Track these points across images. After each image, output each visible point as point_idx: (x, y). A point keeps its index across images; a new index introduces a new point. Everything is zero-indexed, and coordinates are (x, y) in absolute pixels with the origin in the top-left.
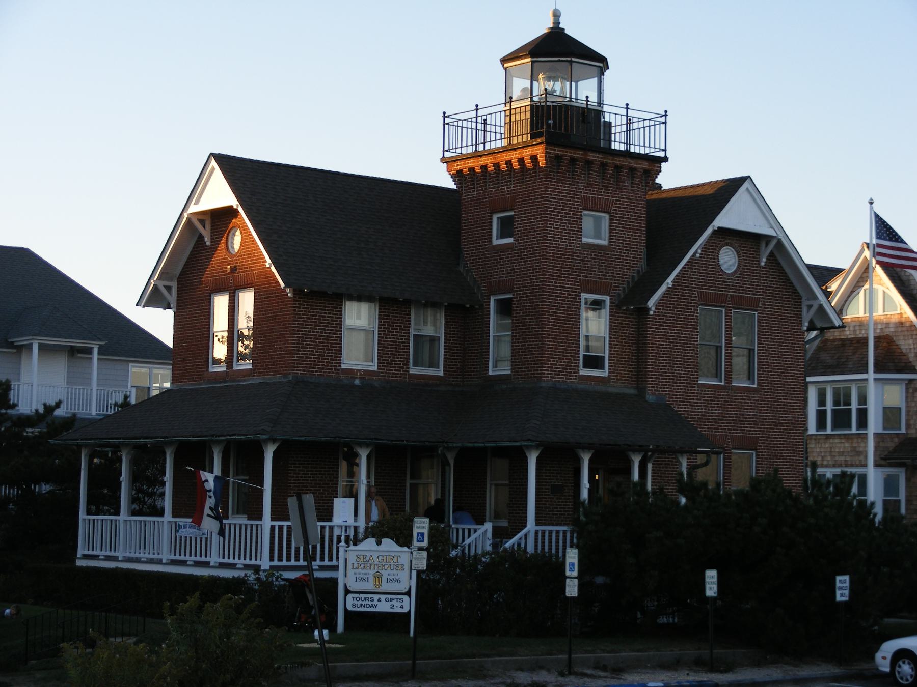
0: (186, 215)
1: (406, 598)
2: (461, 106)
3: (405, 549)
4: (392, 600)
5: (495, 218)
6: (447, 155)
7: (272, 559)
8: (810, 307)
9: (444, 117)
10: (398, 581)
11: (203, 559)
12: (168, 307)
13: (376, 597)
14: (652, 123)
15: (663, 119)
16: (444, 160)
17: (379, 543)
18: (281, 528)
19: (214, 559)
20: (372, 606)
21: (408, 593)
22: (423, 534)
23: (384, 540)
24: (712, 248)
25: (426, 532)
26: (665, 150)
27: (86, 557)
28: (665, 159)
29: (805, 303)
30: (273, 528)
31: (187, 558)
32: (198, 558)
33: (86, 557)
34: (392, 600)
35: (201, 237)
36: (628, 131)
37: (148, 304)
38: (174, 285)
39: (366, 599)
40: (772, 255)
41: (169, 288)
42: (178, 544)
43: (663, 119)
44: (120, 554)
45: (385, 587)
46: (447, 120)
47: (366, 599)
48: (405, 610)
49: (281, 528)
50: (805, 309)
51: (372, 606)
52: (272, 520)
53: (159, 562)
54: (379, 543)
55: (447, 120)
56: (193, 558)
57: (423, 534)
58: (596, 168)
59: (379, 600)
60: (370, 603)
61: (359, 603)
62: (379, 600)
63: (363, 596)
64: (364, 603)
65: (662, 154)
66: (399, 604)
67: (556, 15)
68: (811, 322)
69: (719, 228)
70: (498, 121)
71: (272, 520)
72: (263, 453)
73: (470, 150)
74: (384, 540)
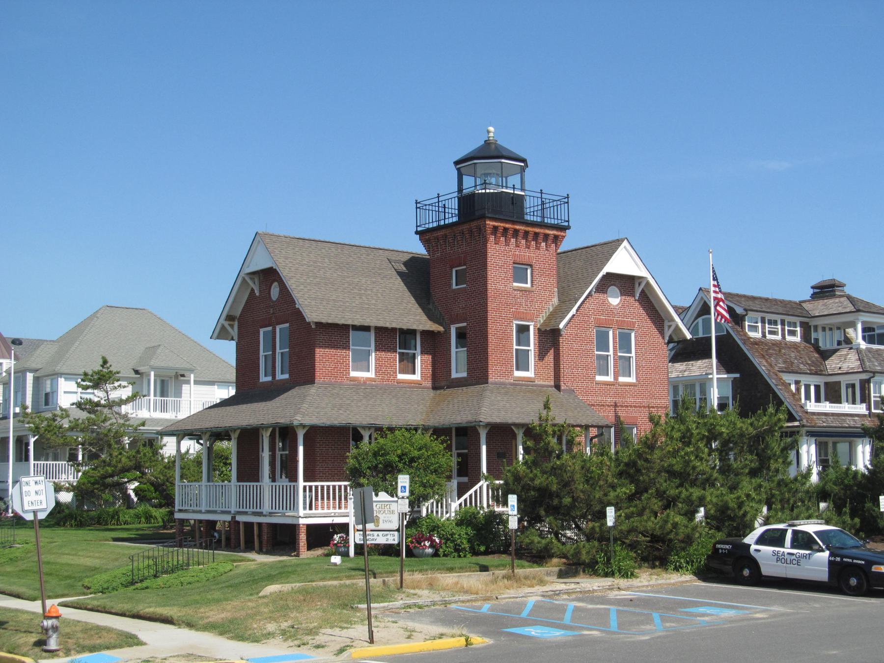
0: (242, 274)
1: (396, 533)
2: (427, 195)
6: (419, 229)
7: (305, 508)
8: (670, 326)
11: (258, 510)
12: (232, 339)
13: (376, 533)
14: (559, 203)
15: (566, 200)
16: (417, 233)
19: (203, 509)
21: (398, 530)
22: (405, 487)
24: (602, 287)
25: (407, 485)
26: (568, 221)
27: (180, 511)
28: (568, 228)
29: (666, 324)
30: (305, 487)
31: (248, 510)
32: (255, 510)
33: (180, 511)
35: (253, 290)
36: (543, 209)
37: (218, 337)
38: (236, 324)
40: (643, 292)
41: (232, 326)
42: (240, 501)
43: (566, 200)
44: (203, 509)
45: (381, 527)
46: (419, 205)
48: (396, 542)
49: (311, 487)
50: (666, 328)
52: (305, 481)
53: (200, 512)
55: (419, 205)
56: (251, 510)
57: (405, 487)
58: (521, 234)
65: (566, 224)
68: (670, 337)
69: (607, 273)
70: (454, 205)
71: (305, 481)
72: (296, 435)
73: (435, 225)
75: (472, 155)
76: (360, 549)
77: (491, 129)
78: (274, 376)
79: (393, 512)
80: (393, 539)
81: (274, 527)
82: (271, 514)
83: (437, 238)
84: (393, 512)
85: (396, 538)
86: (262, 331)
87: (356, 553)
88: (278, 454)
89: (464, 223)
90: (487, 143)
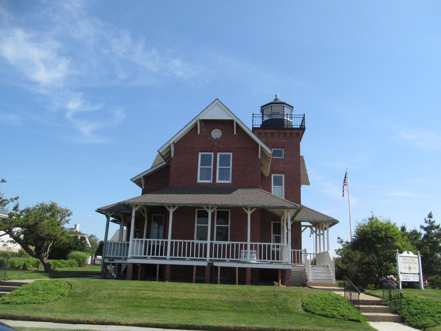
0: (198, 119)
1: (418, 275)
3: (416, 256)
10: (415, 268)
13: (409, 275)
17: (408, 253)
21: (419, 274)
34: (414, 276)
39: (407, 276)
47: (407, 276)
48: (418, 281)
54: (408, 253)
61: (405, 278)
63: (405, 275)
64: (406, 278)
78: (214, 179)
79: (415, 263)
84: (415, 263)
85: (418, 278)
86: (200, 154)
88: (216, 226)
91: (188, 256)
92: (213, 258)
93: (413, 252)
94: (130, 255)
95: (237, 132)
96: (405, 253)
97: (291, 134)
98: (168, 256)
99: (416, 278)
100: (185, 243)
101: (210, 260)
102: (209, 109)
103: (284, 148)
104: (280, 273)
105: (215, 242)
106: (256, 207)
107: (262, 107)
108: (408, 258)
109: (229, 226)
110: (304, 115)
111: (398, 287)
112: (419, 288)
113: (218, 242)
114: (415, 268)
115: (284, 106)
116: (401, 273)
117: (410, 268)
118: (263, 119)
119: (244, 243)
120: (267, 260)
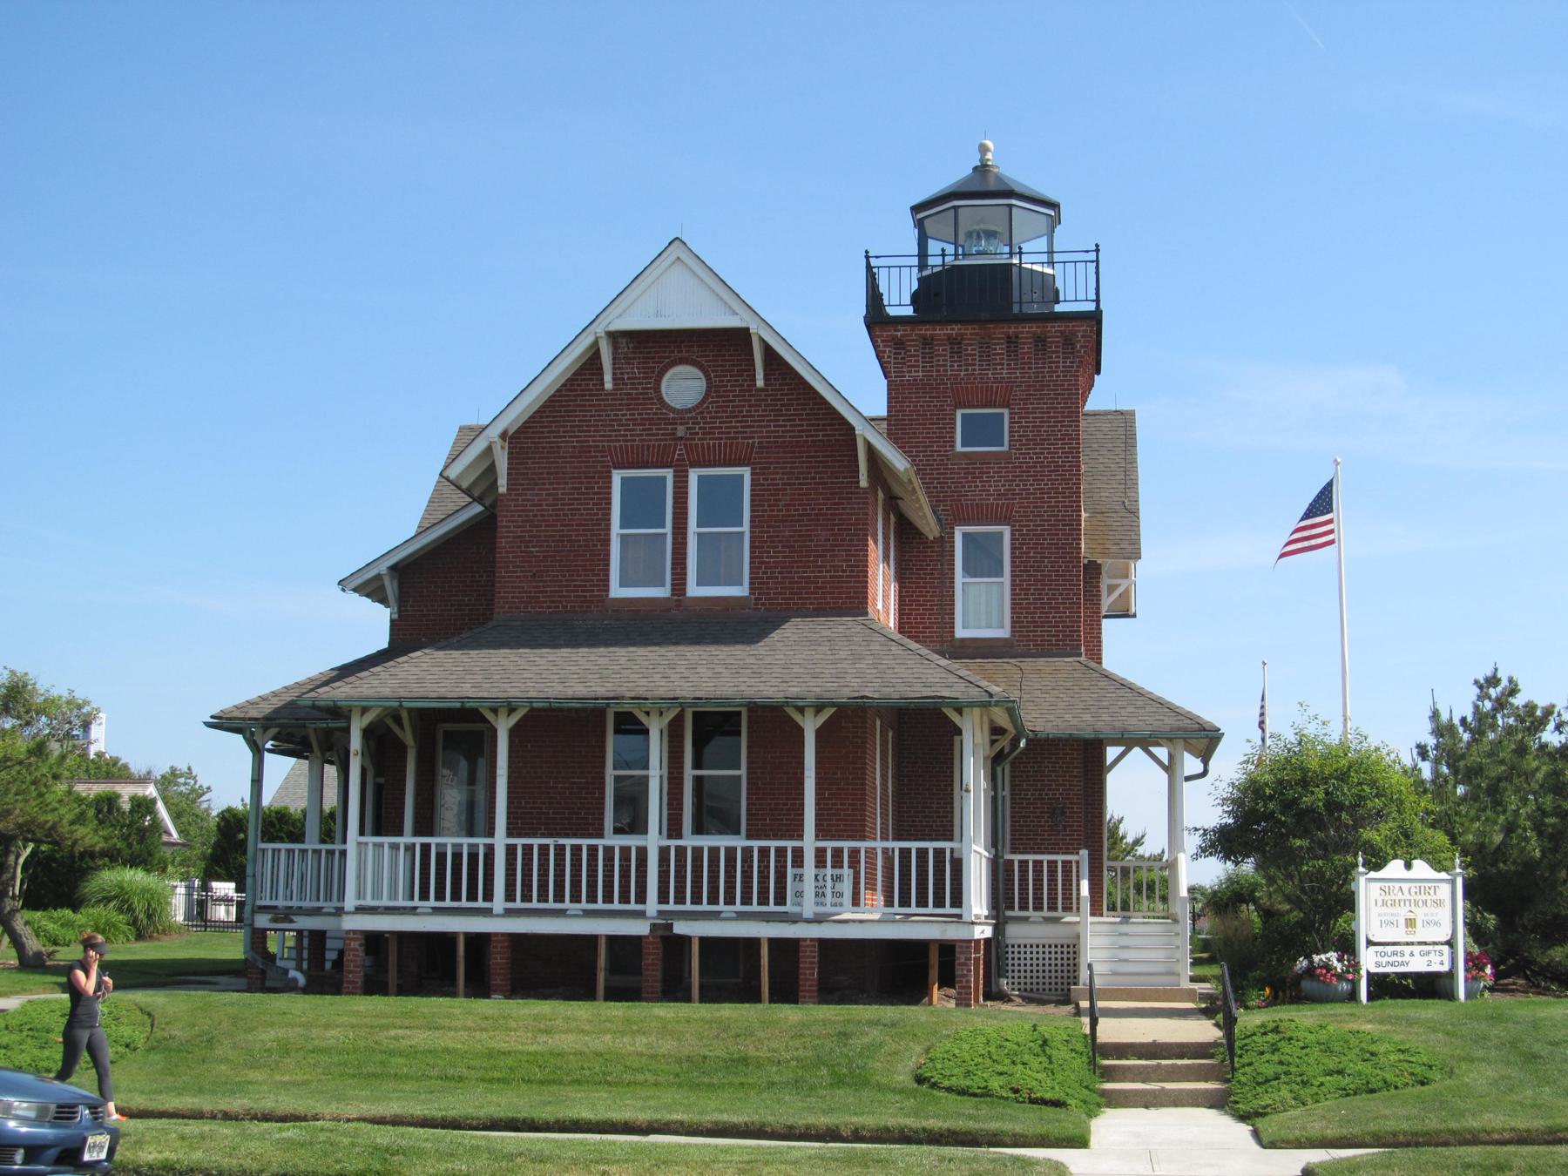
0: (599, 329)
1: (1446, 948)
3: (1443, 875)
4: (1429, 953)
5: (959, 413)
9: (867, 257)
10: (1436, 923)
13: (1407, 949)
17: (1408, 866)
18: (764, 852)
20: (1402, 964)
21: (1450, 943)
23: (1415, 862)
34: (1429, 953)
47: (1395, 953)
48: (1445, 968)
51: (1402, 964)
54: (1408, 866)
59: (1412, 954)
60: (1400, 959)
62: (1412, 954)
63: (1389, 949)
64: (1391, 959)
66: (1438, 959)
67: (983, 149)
74: (1415, 862)
75: (964, 189)
76: (1384, 987)
77: (990, 144)
79: (1438, 903)
80: (1437, 962)
81: (824, 943)
82: (819, 919)
83: (928, 342)
84: (1438, 903)
86: (617, 477)
87: (1370, 997)
89: (923, 322)
90: (982, 169)
91: (576, 898)
92: (672, 906)
93: (1428, 861)
94: (350, 902)
95: (766, 378)
96: (1395, 868)
97: (1040, 341)
98: (499, 903)
99: (1435, 958)
100: (560, 850)
101: (660, 912)
102: (650, 279)
103: (1007, 406)
104: (934, 959)
105: (690, 841)
106: (833, 705)
107: (916, 209)
108: (1405, 886)
109: (743, 772)
110: (1097, 251)
111: (1353, 996)
112: (1450, 995)
113: (706, 842)
114: (1436, 923)
115: (1010, 206)
116: (1370, 943)
117: (1410, 923)
118: (922, 265)
119: (789, 844)
120: (1031, 913)
